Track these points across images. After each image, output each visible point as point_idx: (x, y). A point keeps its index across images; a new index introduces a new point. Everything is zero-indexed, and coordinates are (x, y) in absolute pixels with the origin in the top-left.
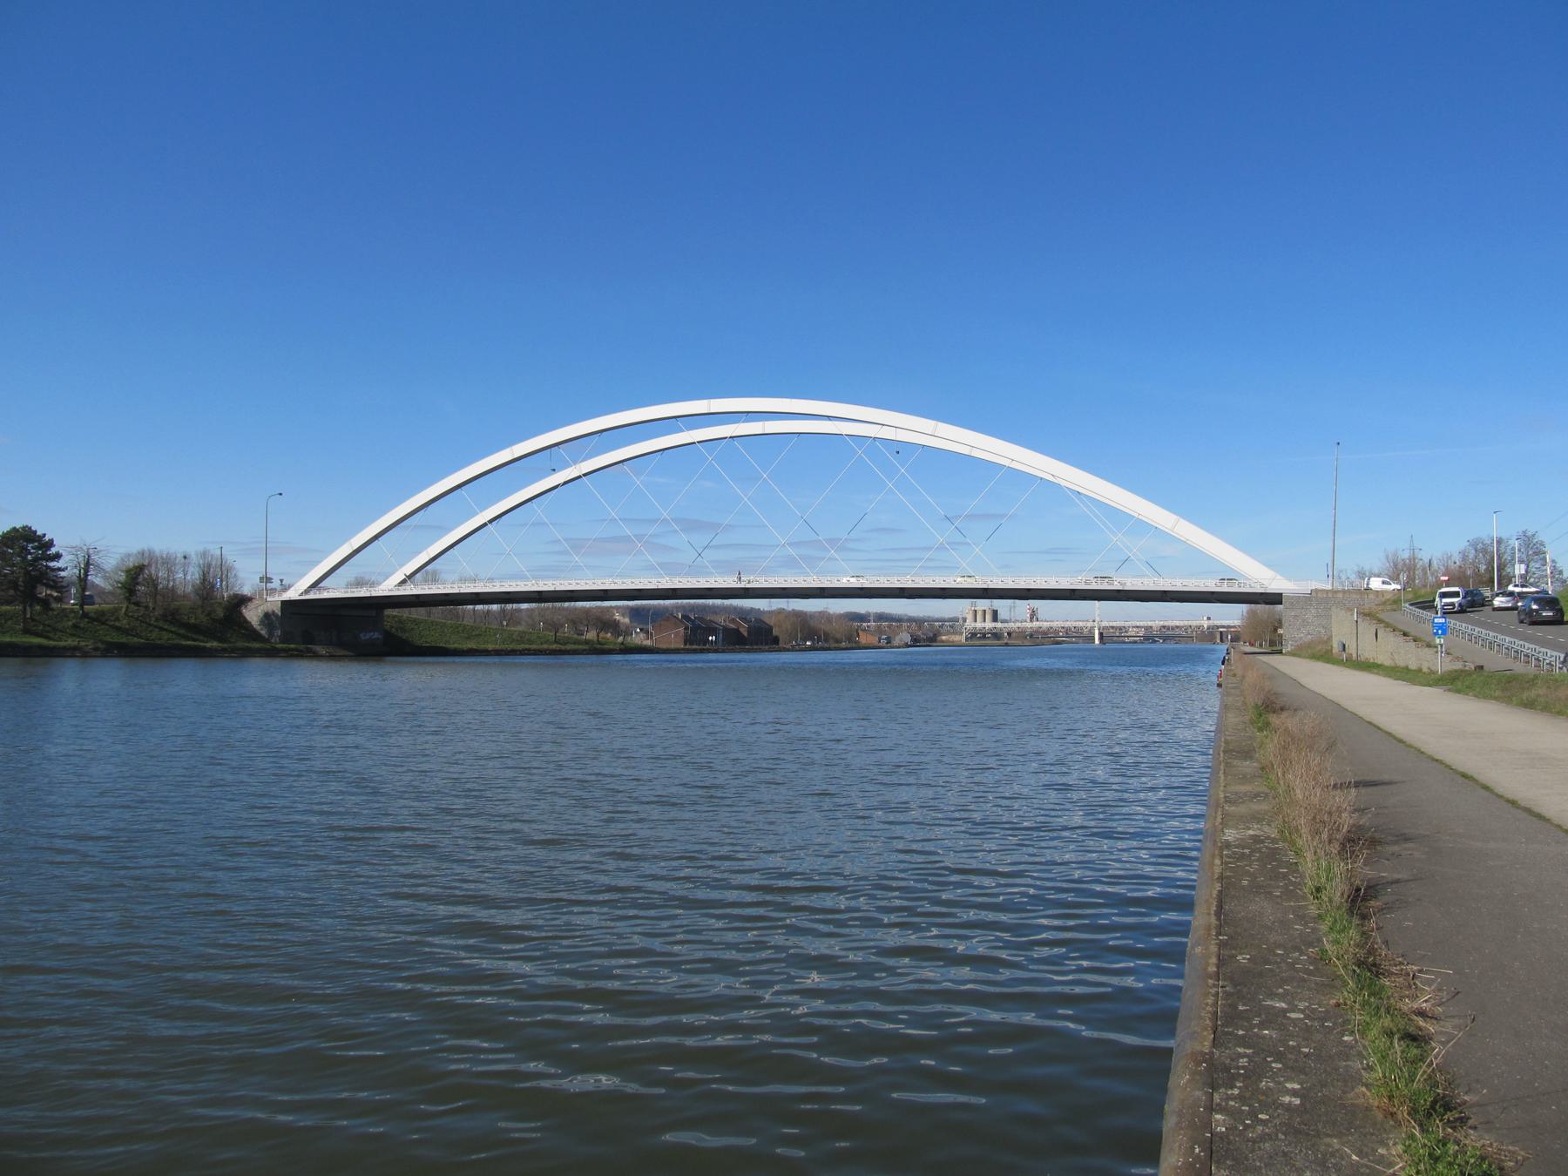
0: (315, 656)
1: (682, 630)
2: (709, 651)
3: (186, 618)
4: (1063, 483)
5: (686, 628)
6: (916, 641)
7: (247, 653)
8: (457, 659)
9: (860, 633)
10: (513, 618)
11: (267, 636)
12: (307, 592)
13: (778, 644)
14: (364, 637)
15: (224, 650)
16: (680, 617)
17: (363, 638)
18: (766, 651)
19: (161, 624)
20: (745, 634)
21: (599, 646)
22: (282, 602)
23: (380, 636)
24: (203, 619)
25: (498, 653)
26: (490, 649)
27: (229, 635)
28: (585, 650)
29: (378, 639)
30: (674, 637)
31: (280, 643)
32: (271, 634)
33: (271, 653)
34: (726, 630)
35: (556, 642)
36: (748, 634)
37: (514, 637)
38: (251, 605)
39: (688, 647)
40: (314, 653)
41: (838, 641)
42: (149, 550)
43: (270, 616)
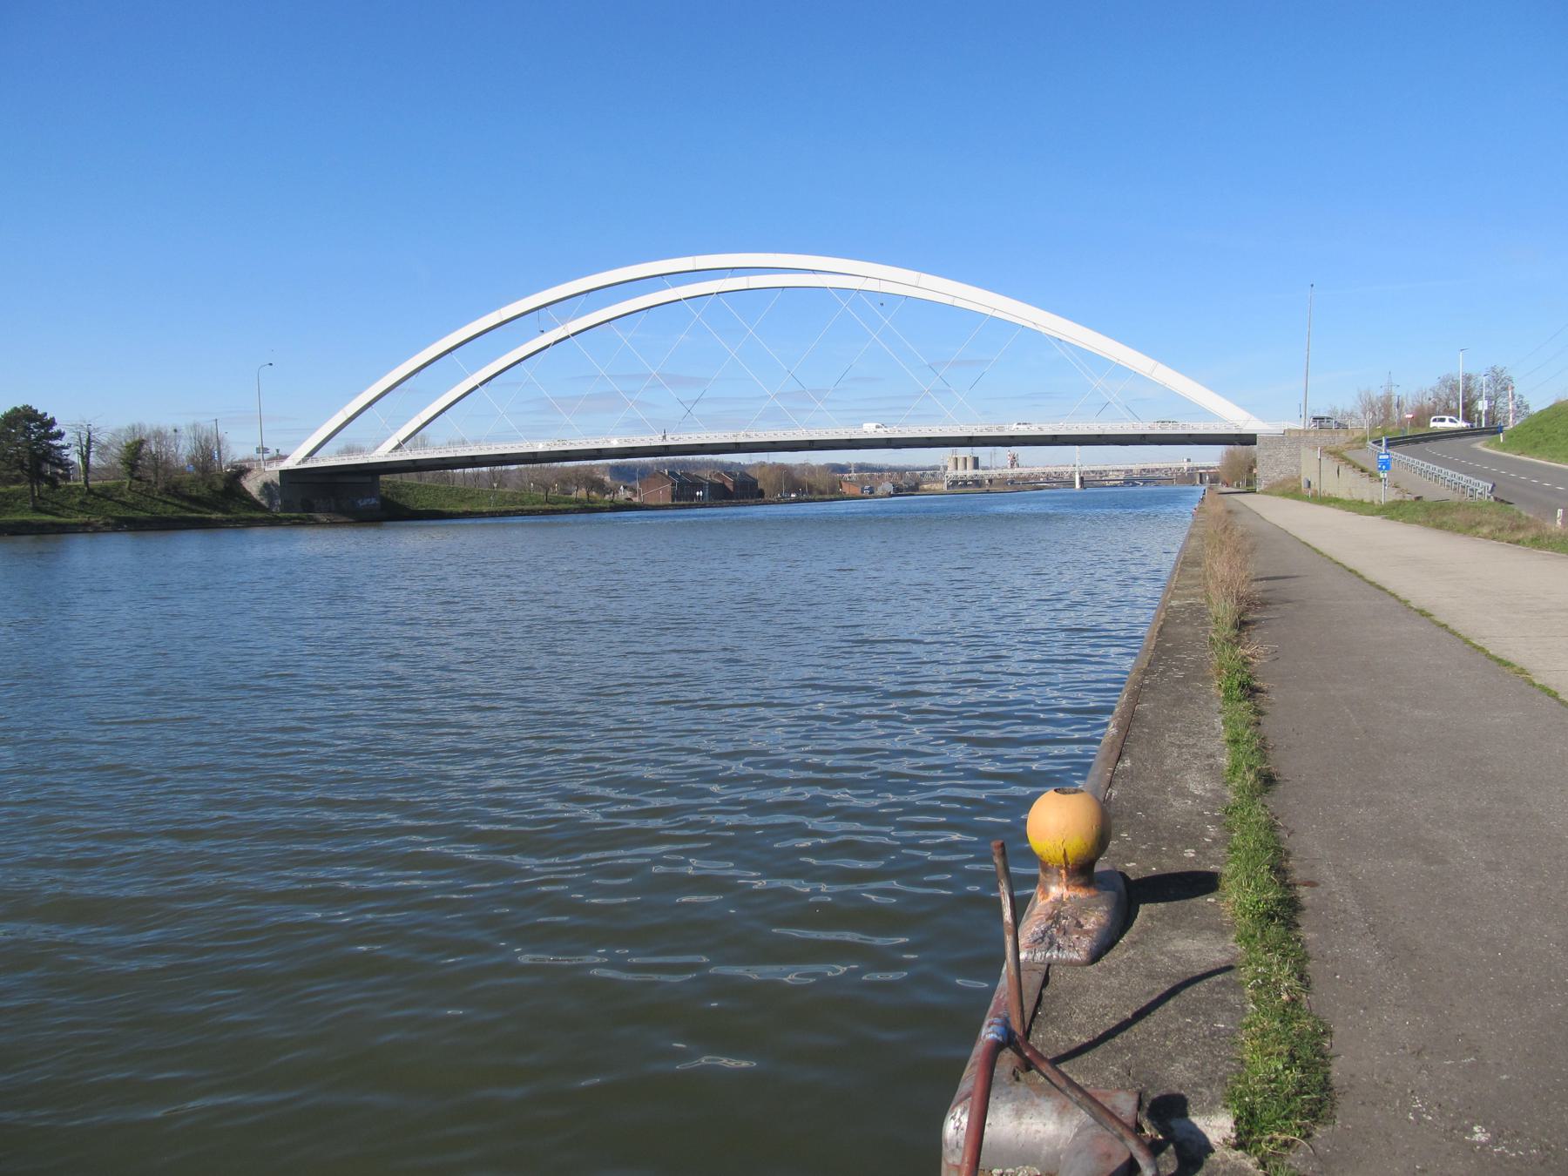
0: (317, 523)
1: (669, 486)
2: (696, 506)
3: (188, 490)
4: (1044, 331)
5: (673, 485)
6: (898, 491)
7: (252, 523)
8: (479, 521)
9: (843, 483)
10: (502, 480)
11: (267, 506)
12: (304, 460)
13: (763, 497)
14: (362, 503)
15: (229, 521)
18: (753, 505)
19: (164, 498)
20: (731, 488)
21: (590, 505)
22: (281, 471)
24: (204, 491)
25: (492, 515)
27: (231, 506)
28: (575, 509)
29: (374, 505)
30: (662, 494)
31: (282, 511)
32: (271, 503)
33: (274, 522)
34: (711, 484)
35: (547, 502)
37: (507, 499)
38: (250, 476)
39: (676, 502)
40: (315, 520)
41: (821, 493)
42: (139, 424)
43: (269, 485)
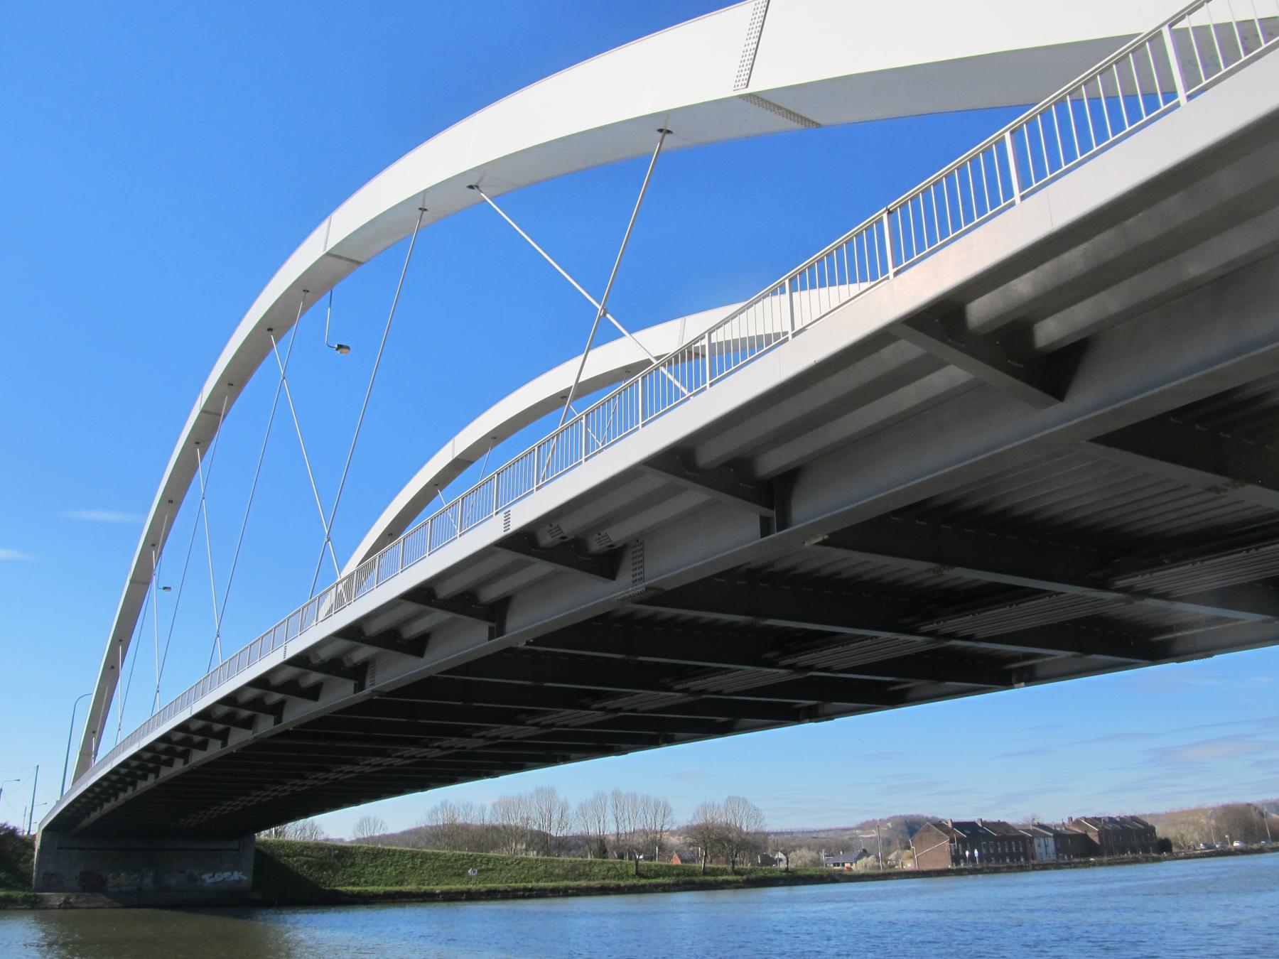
1: (946, 842)
5: (952, 841)
16: (950, 825)
20: (1096, 840)
26: (438, 892)
29: (240, 881)
35: (639, 874)
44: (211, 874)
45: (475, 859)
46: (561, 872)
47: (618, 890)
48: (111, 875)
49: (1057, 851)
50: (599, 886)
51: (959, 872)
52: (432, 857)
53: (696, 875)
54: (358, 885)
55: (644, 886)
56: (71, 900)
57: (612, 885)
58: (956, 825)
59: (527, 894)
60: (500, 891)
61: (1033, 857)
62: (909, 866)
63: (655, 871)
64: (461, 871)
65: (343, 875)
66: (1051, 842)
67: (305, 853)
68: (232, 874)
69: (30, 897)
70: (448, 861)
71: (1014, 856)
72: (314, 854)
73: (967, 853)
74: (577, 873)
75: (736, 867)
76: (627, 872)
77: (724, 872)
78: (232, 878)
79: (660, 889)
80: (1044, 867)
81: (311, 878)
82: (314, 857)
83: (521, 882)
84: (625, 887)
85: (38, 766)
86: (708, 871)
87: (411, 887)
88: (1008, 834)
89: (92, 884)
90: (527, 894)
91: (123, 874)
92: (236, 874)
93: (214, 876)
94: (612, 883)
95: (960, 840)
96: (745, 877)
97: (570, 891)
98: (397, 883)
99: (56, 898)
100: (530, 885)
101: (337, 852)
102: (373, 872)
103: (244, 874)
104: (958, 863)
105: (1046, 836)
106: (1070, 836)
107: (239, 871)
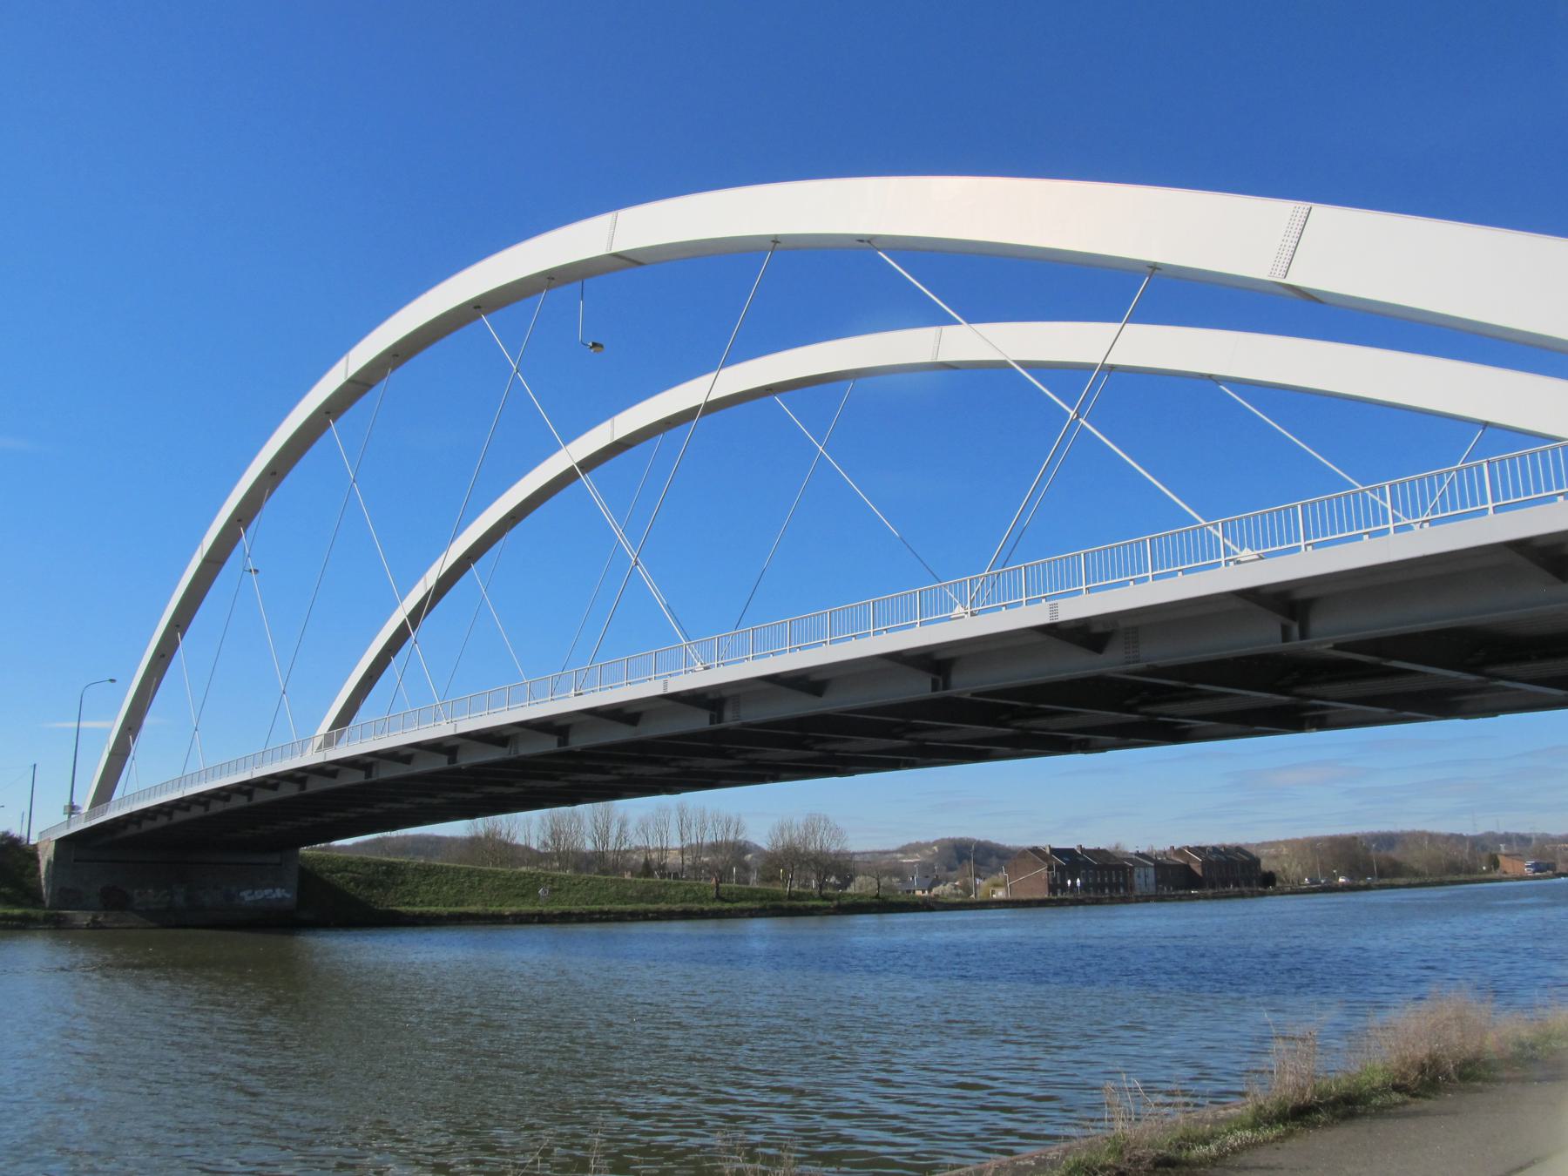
1: (1043, 870)
5: (1050, 869)
16: (1048, 851)
17: (248, 899)
20: (1199, 871)
23: (288, 896)
26: (507, 913)
29: (282, 899)
35: (719, 898)
36: (1203, 872)
41: (1416, 874)
44: (250, 891)
45: (538, 878)
46: (635, 894)
47: (702, 915)
48: (136, 891)
49: (1157, 882)
50: (680, 909)
51: (1061, 903)
52: (490, 875)
53: (780, 899)
54: (414, 905)
55: (729, 910)
56: (100, 919)
57: (695, 909)
58: (1054, 851)
59: (604, 917)
60: (574, 914)
61: (1132, 888)
62: (1000, 894)
63: (737, 894)
64: (524, 891)
65: (396, 893)
66: (1151, 872)
67: (349, 868)
68: (274, 891)
69: (52, 916)
70: (509, 879)
71: (1114, 887)
72: (360, 871)
73: (1069, 882)
74: (652, 894)
75: (823, 892)
76: (706, 895)
77: (810, 896)
78: (274, 896)
79: (746, 914)
80: (1147, 899)
81: (360, 897)
82: (360, 873)
83: (592, 904)
84: (709, 911)
85: (35, 765)
86: (793, 895)
87: (473, 909)
88: (1110, 863)
89: (114, 900)
90: (604, 917)
91: (150, 891)
92: (278, 890)
93: (253, 893)
94: (696, 906)
95: (1059, 867)
96: (836, 902)
97: (650, 915)
98: (457, 905)
99: (82, 918)
100: (606, 907)
101: (384, 868)
102: (427, 891)
103: (287, 892)
104: (1055, 893)
105: (1146, 866)
106: (1170, 866)
107: (282, 888)
